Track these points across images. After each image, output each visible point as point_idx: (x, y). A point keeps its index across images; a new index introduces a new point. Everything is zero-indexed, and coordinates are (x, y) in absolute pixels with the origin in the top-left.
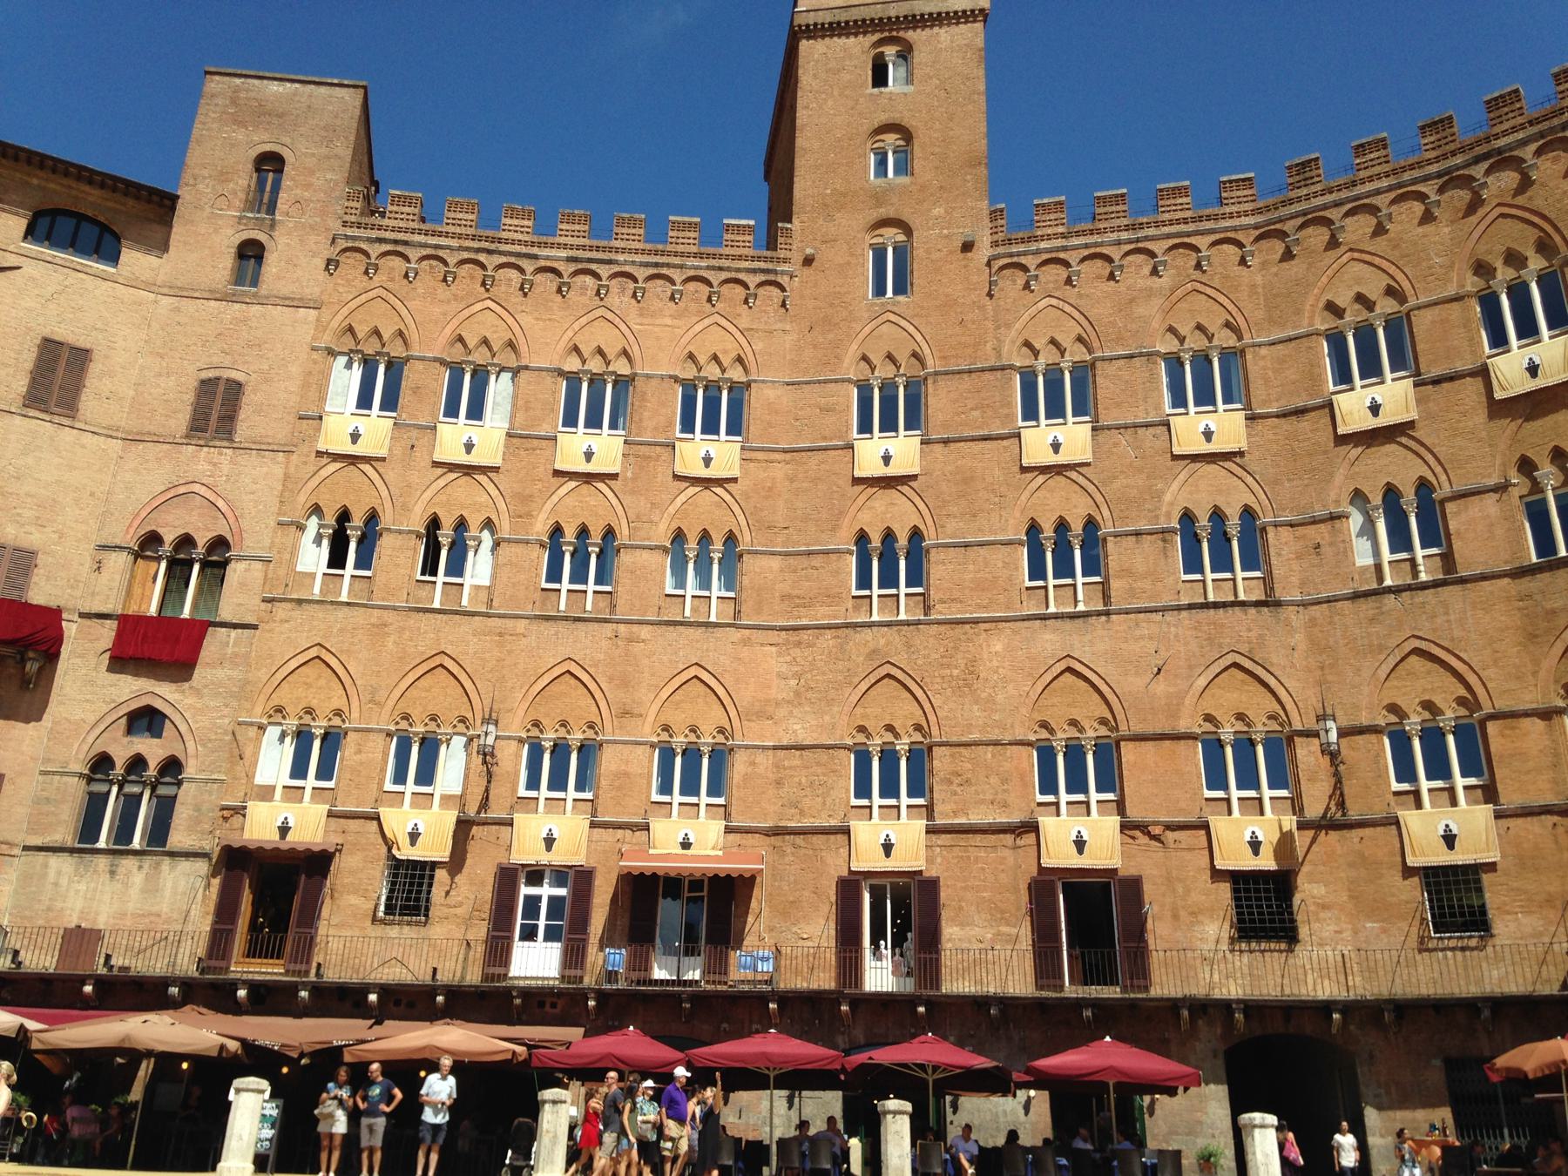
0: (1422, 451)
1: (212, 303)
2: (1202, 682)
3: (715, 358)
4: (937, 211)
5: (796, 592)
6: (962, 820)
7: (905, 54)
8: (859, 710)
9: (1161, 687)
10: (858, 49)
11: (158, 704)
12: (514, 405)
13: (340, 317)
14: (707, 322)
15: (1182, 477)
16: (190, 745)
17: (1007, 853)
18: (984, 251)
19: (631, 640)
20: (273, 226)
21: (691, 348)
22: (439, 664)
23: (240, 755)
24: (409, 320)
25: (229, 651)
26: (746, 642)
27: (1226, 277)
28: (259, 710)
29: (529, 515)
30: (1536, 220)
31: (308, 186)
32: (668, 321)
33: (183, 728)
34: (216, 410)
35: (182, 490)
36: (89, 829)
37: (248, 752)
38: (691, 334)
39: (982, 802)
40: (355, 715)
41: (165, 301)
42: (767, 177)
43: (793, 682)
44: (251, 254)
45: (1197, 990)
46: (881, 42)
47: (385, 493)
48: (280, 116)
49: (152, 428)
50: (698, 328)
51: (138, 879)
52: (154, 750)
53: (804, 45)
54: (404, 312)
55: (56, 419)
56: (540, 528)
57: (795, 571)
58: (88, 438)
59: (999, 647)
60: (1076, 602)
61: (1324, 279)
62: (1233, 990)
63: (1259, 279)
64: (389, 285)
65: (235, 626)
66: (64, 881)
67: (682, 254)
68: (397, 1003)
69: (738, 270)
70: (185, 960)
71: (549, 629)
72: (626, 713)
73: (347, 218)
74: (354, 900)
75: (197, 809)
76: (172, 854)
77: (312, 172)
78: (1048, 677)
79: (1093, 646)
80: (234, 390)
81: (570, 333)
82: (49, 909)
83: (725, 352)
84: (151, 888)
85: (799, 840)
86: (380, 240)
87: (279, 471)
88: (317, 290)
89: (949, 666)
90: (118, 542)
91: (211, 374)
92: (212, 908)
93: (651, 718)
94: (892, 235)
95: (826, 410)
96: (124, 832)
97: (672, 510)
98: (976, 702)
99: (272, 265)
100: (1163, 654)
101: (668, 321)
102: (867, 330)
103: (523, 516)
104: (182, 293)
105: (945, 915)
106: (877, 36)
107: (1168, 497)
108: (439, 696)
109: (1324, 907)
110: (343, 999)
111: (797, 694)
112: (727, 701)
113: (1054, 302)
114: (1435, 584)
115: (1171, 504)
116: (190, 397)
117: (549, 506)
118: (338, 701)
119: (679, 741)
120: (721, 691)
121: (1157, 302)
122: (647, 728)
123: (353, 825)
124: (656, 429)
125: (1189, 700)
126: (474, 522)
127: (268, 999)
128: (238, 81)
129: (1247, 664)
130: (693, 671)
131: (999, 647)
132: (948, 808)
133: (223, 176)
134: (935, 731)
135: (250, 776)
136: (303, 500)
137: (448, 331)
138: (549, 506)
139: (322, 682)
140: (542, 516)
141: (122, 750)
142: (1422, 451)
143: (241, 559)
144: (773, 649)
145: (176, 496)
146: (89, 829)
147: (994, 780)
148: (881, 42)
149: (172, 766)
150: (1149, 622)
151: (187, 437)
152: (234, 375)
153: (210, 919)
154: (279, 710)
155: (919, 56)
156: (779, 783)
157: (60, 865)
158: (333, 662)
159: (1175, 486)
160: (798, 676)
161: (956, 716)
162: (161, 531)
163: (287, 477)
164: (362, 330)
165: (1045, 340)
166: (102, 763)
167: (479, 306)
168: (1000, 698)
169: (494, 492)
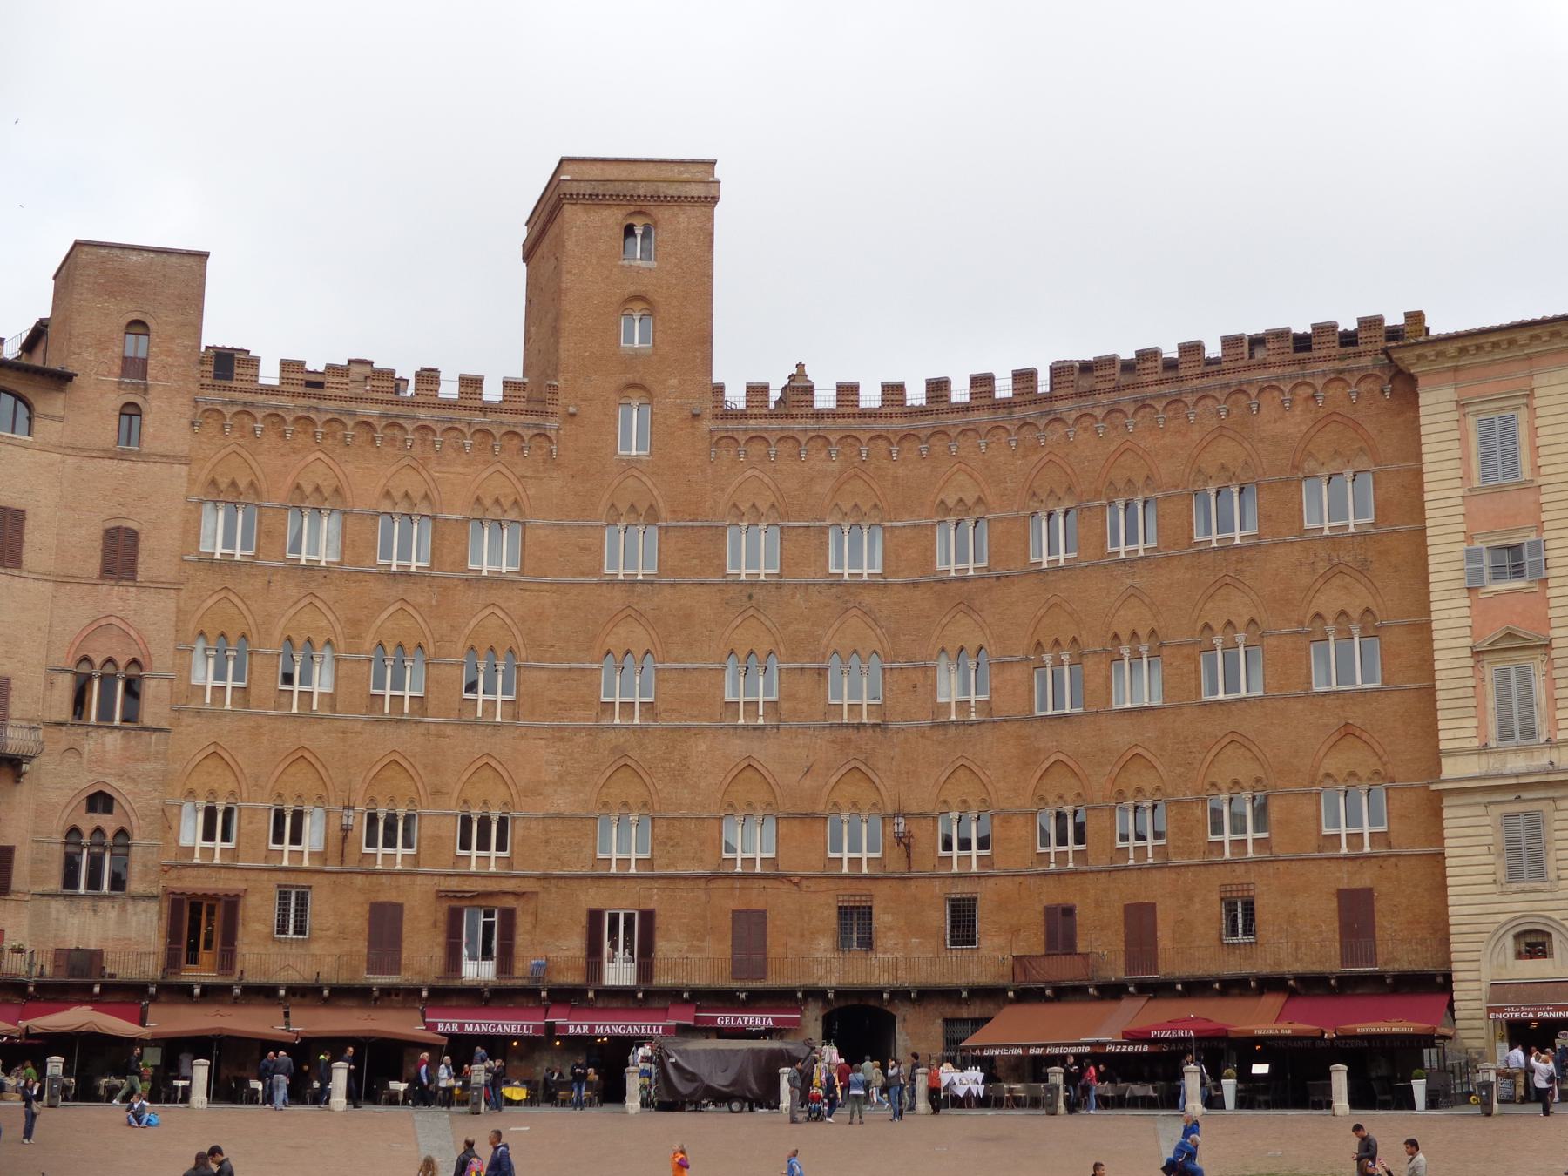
1: (107, 462)
2: (834, 779)
3: (497, 501)
4: (673, 382)
6: (671, 872)
8: (605, 791)
9: (808, 783)
10: (613, 218)
11: (107, 790)
12: (343, 543)
13: (206, 471)
14: (492, 469)
15: (836, 626)
16: (134, 820)
18: (707, 424)
19: (439, 736)
20: (146, 389)
21: (479, 492)
22: (300, 757)
24: (259, 472)
25: (153, 749)
26: (523, 737)
27: (878, 468)
28: (178, 793)
29: (359, 636)
31: (170, 353)
32: (461, 470)
33: (127, 807)
34: (120, 554)
35: (103, 622)
36: (70, 880)
37: (174, 824)
38: (478, 481)
40: (245, 795)
41: (70, 460)
42: (527, 258)
45: (809, 981)
46: (632, 214)
47: (251, 621)
48: (142, 285)
49: (74, 571)
50: (485, 475)
51: (113, 915)
52: (109, 823)
53: (568, 210)
54: (254, 465)
55: (9, 571)
56: (369, 643)
58: (31, 584)
59: (703, 747)
60: (758, 716)
62: (830, 979)
63: (900, 472)
64: (242, 441)
65: (155, 730)
66: (63, 917)
67: (471, 409)
68: (294, 995)
69: (515, 425)
70: (150, 968)
71: (380, 729)
72: (437, 792)
73: (205, 381)
74: (258, 927)
75: (145, 865)
76: (133, 898)
77: (172, 339)
78: (735, 772)
79: (765, 752)
80: (133, 535)
81: (383, 481)
82: (56, 936)
83: (506, 496)
84: (122, 922)
85: (561, 883)
86: (233, 402)
87: (172, 605)
88: (186, 448)
89: (668, 760)
90: (62, 665)
91: (113, 524)
92: (164, 933)
93: (455, 796)
95: (585, 549)
96: (94, 882)
97: (467, 631)
100: (811, 759)
101: (461, 470)
102: (616, 482)
104: (81, 451)
105: (658, 934)
107: (825, 641)
109: (891, 929)
110: (263, 993)
111: (560, 777)
112: (509, 782)
113: (756, 473)
114: (981, 722)
115: (827, 647)
116: (99, 544)
117: (373, 629)
118: (231, 786)
119: (476, 814)
120: (505, 775)
122: (453, 803)
123: (252, 875)
124: (453, 563)
125: (826, 791)
126: (319, 640)
127: (214, 994)
128: (104, 252)
129: (863, 768)
130: (485, 760)
131: (703, 747)
132: (664, 861)
133: (102, 344)
134: (657, 807)
135: (177, 841)
136: (192, 627)
137: (289, 480)
138: (373, 629)
139: (219, 771)
140: (369, 638)
141: (87, 823)
144: (543, 742)
145: (100, 627)
147: (695, 843)
148: (632, 214)
149: (122, 832)
151: (101, 578)
152: (130, 524)
153: (163, 941)
154: (191, 792)
155: (661, 235)
156: (547, 842)
157: (57, 906)
158: (226, 756)
159: (830, 632)
160: (561, 764)
162: (92, 655)
163: (179, 610)
164: (224, 483)
165: (748, 505)
166: (74, 831)
167: (311, 458)
168: (702, 785)
169: (332, 618)
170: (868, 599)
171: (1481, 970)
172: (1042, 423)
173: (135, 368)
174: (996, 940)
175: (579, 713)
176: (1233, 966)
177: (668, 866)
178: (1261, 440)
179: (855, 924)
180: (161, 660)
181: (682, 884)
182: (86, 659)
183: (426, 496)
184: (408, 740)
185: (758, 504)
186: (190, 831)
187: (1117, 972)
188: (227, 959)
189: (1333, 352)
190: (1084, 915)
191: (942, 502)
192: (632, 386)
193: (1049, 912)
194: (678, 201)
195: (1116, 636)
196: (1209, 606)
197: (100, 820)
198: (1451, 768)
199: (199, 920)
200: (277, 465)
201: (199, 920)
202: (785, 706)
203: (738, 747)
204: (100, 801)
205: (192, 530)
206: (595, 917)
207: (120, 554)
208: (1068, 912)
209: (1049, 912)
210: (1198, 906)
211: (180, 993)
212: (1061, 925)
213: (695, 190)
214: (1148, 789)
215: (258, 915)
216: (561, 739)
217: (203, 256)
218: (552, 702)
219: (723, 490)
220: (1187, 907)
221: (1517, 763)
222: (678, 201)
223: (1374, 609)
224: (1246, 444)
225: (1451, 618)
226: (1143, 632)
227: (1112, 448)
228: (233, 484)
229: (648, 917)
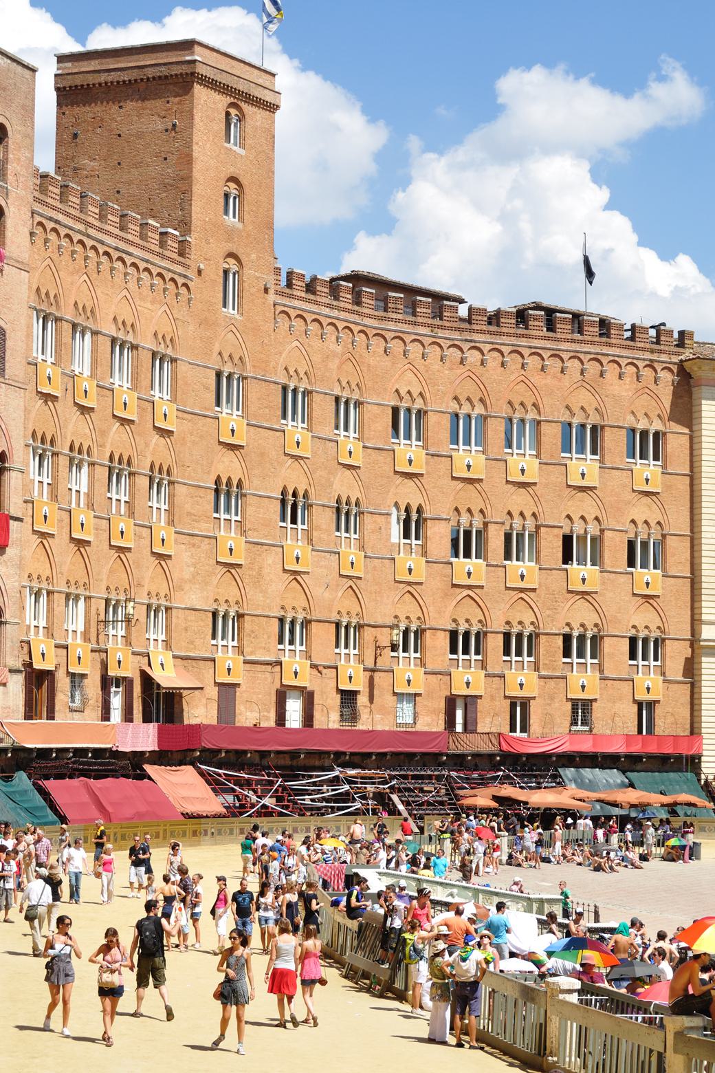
0: (423, 490)
5: (193, 511)
7: (241, 118)
10: (221, 102)
17: (268, 675)
18: (272, 297)
30: (482, 387)
39: (260, 648)
43: (192, 569)
57: (192, 497)
59: (270, 561)
61: (397, 376)
89: (252, 569)
94: (232, 265)
98: (261, 592)
106: (230, 100)
113: (298, 344)
118: (48, 573)
121: (337, 361)
131: (270, 561)
142: (423, 490)
143: (15, 470)
147: (265, 636)
150: (325, 557)
160: (194, 565)
164: (43, 291)
172: (465, 346)
174: (426, 718)
175: (204, 525)
177: (252, 653)
178: (607, 396)
181: (259, 667)
183: (132, 325)
185: (299, 370)
189: (648, 346)
191: (397, 391)
192: (231, 255)
195: (509, 513)
196: (570, 503)
202: (315, 534)
210: (557, 705)
213: (268, 99)
214: (527, 623)
216: (194, 545)
217: (34, 70)
218: (189, 514)
219: (281, 354)
220: (550, 705)
223: (662, 522)
224: (597, 396)
226: (528, 514)
227: (513, 378)
228: (47, 294)
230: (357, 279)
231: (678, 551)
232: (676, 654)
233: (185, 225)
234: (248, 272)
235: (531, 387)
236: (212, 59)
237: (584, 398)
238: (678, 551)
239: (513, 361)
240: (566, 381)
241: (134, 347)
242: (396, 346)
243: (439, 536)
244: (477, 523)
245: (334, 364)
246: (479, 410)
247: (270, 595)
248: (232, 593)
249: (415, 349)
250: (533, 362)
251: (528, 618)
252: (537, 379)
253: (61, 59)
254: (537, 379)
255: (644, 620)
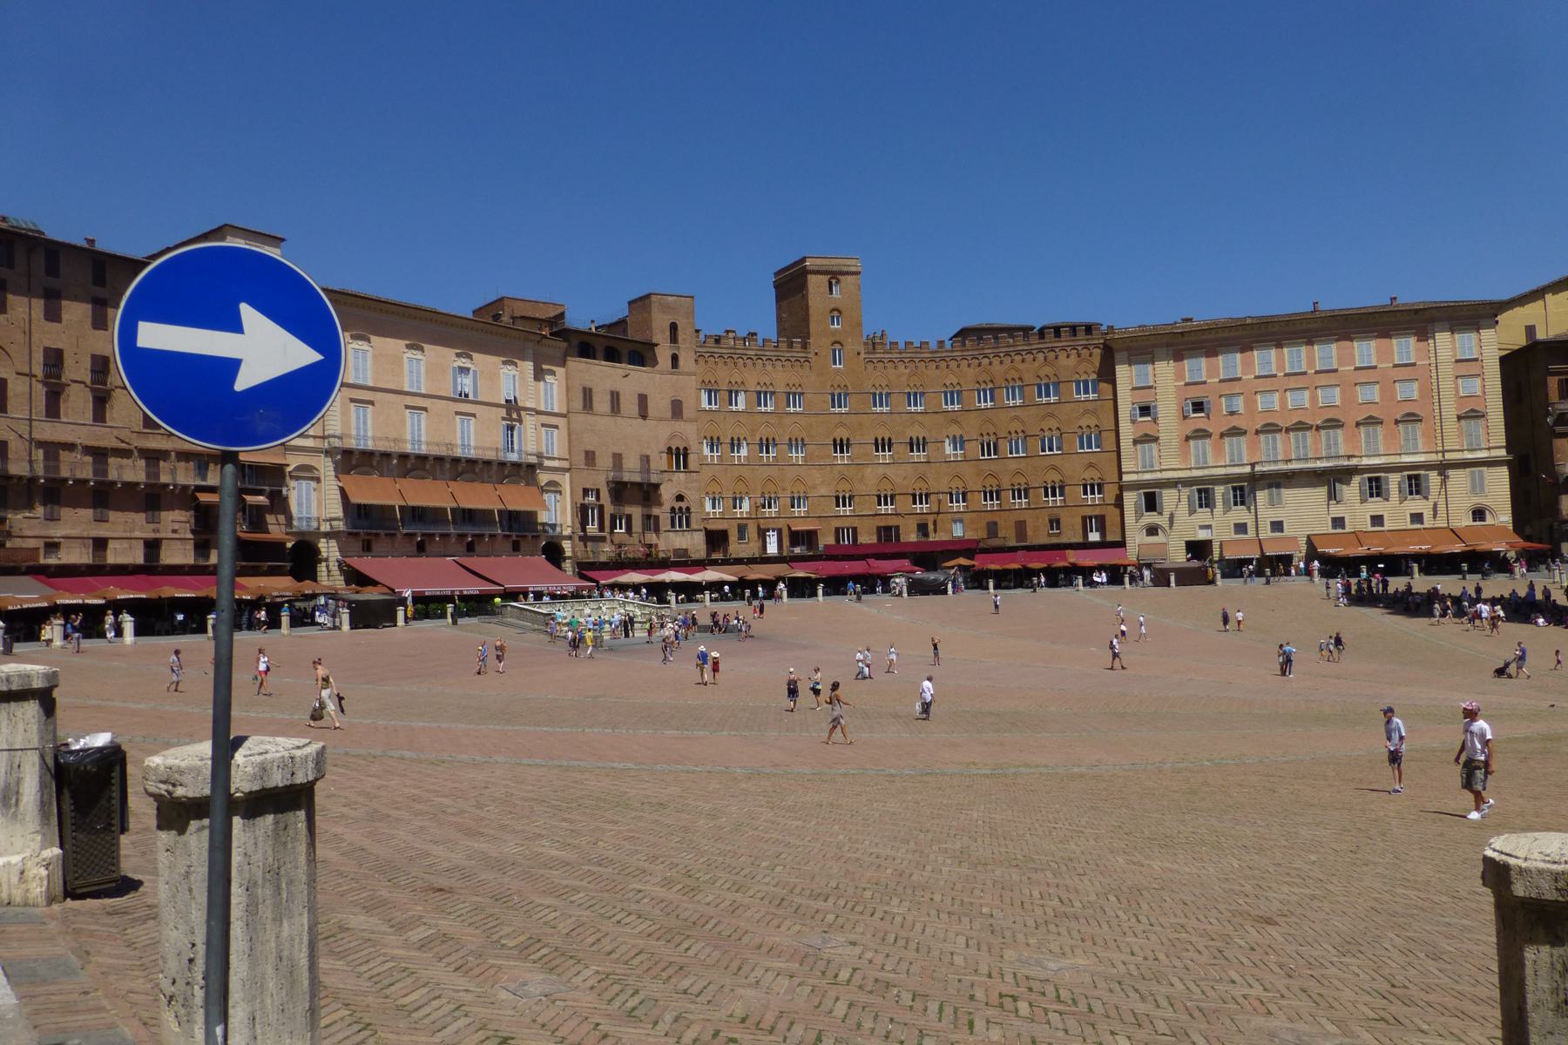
7: (838, 282)
10: (825, 278)
18: (863, 355)
22: (740, 479)
23: (702, 506)
34: (677, 409)
36: (673, 525)
44: (675, 358)
52: (683, 505)
79: (890, 471)
99: (681, 362)
103: (753, 436)
108: (741, 487)
110: (739, 561)
141: (677, 505)
145: (673, 436)
146: (673, 525)
155: (843, 284)
161: (860, 488)
166: (673, 509)
170: (920, 418)
171: (1137, 540)
173: (674, 339)
176: (1055, 540)
179: (923, 528)
180: (693, 448)
182: (670, 449)
184: (773, 471)
186: (708, 507)
187: (1012, 543)
188: (726, 551)
190: (1001, 523)
193: (988, 524)
194: (847, 273)
197: (680, 504)
198: (1126, 478)
199: (716, 539)
200: (724, 375)
201: (716, 539)
203: (881, 470)
204: (680, 498)
205: (699, 400)
206: (837, 530)
207: (677, 409)
208: (995, 523)
209: (988, 524)
211: (714, 563)
212: (992, 529)
215: (733, 536)
221: (1148, 476)
222: (847, 273)
225: (1127, 431)
229: (855, 530)
230: (964, 333)
231: (1109, 438)
232: (1111, 492)
233: (805, 336)
234: (848, 348)
235: (1017, 370)
236: (818, 262)
237: (1047, 370)
238: (1109, 438)
239: (1007, 360)
240: (1036, 364)
241: (773, 393)
242: (943, 364)
243: (974, 449)
244: (993, 439)
245: (904, 379)
246: (1019, 383)
247: (869, 482)
248: (847, 487)
249: (953, 364)
250: (1018, 358)
251: (1023, 481)
252: (1021, 366)
253: (777, 274)
254: (1021, 366)
255: (1091, 475)
